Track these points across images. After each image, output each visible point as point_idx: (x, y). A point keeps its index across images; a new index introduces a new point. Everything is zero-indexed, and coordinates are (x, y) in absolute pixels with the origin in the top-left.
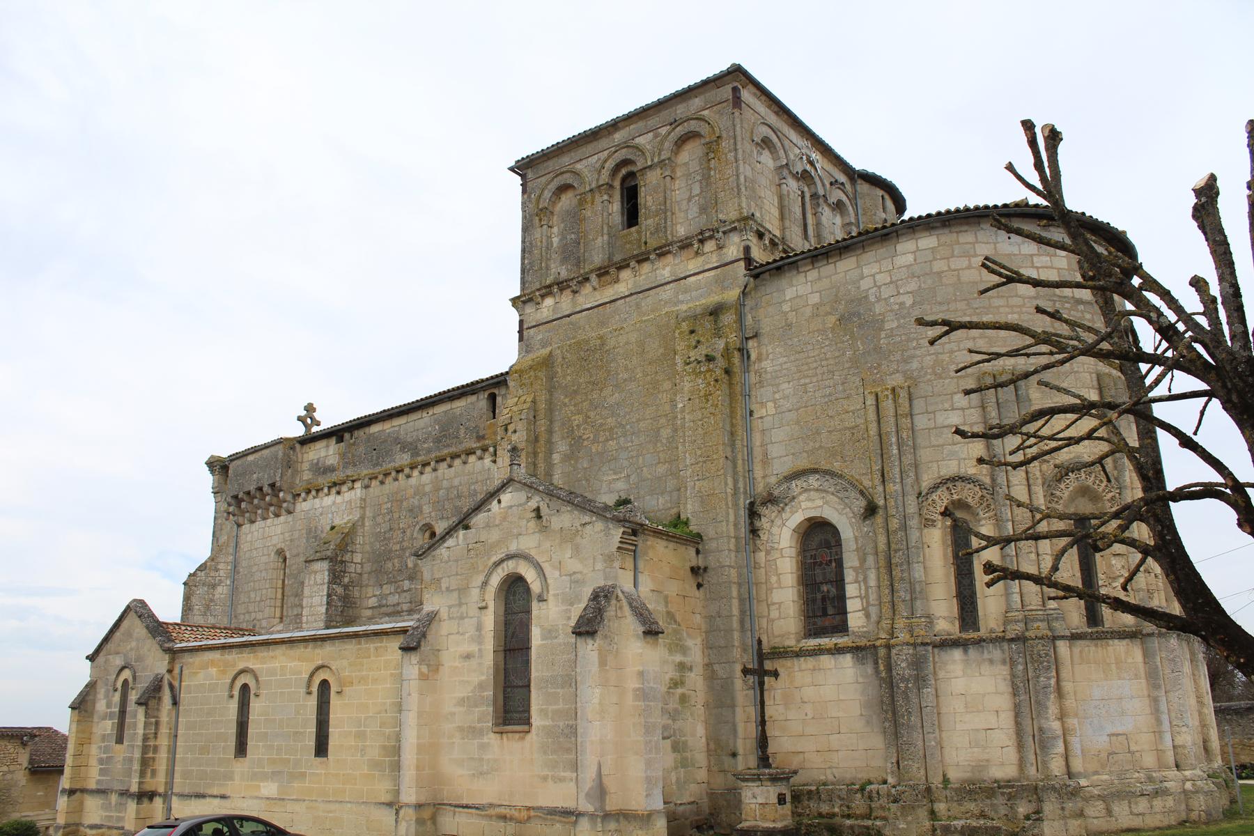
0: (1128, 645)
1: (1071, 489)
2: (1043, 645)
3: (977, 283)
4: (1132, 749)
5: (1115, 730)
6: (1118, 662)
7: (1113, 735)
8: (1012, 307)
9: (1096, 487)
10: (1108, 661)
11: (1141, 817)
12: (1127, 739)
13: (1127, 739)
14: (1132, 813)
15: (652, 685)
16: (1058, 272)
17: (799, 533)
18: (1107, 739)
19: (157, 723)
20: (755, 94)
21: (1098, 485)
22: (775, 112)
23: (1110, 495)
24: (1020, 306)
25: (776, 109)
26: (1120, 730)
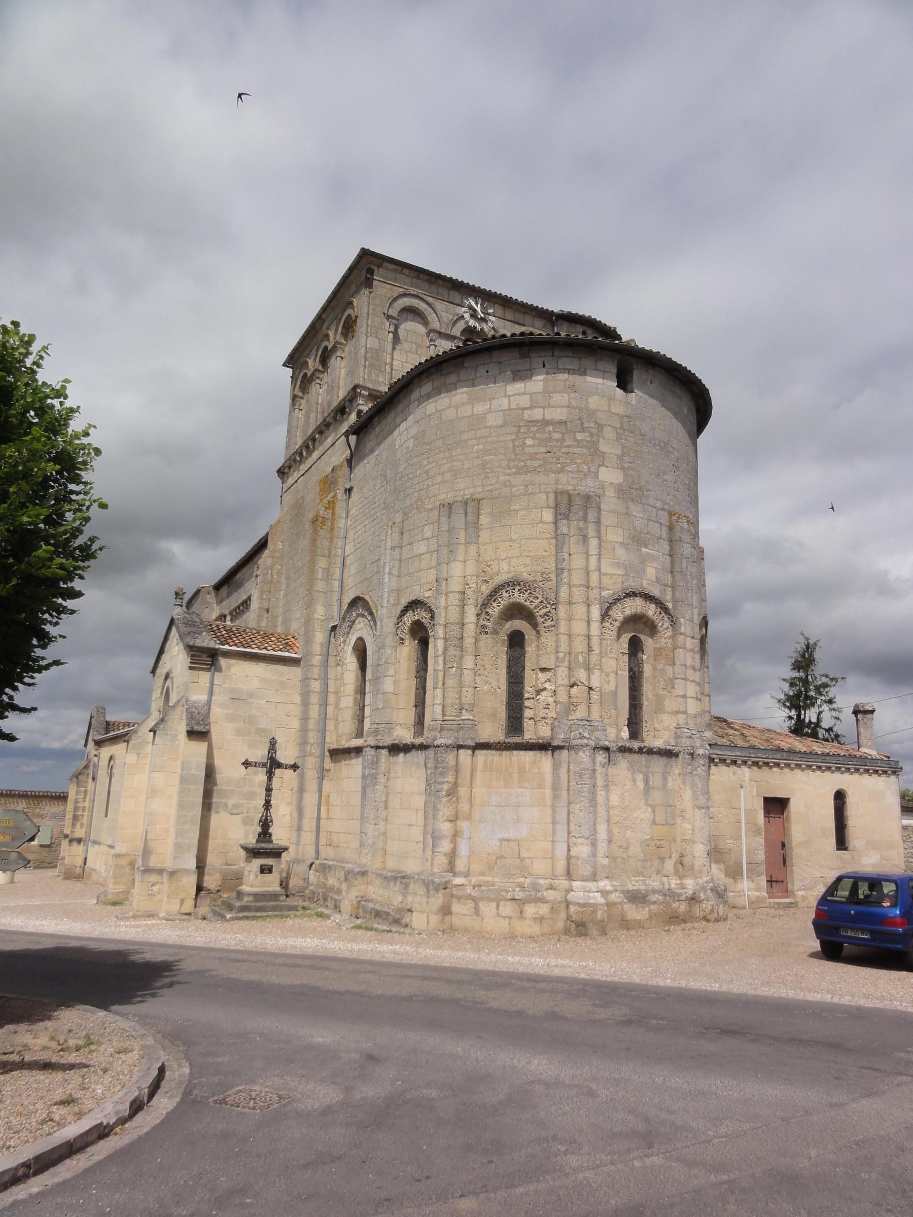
0: (535, 755)
1: (502, 607)
2: (441, 752)
3: (452, 421)
4: (521, 854)
5: (506, 836)
6: (521, 771)
7: (505, 840)
8: (480, 438)
9: (528, 603)
10: (511, 770)
11: (507, 920)
12: (519, 845)
13: (519, 845)
14: (498, 915)
15: (193, 772)
16: (531, 396)
17: (358, 650)
18: (498, 843)
19: (86, 792)
20: (395, 271)
21: (532, 602)
22: (427, 280)
23: (544, 611)
24: (486, 437)
25: (426, 277)
26: (512, 835)
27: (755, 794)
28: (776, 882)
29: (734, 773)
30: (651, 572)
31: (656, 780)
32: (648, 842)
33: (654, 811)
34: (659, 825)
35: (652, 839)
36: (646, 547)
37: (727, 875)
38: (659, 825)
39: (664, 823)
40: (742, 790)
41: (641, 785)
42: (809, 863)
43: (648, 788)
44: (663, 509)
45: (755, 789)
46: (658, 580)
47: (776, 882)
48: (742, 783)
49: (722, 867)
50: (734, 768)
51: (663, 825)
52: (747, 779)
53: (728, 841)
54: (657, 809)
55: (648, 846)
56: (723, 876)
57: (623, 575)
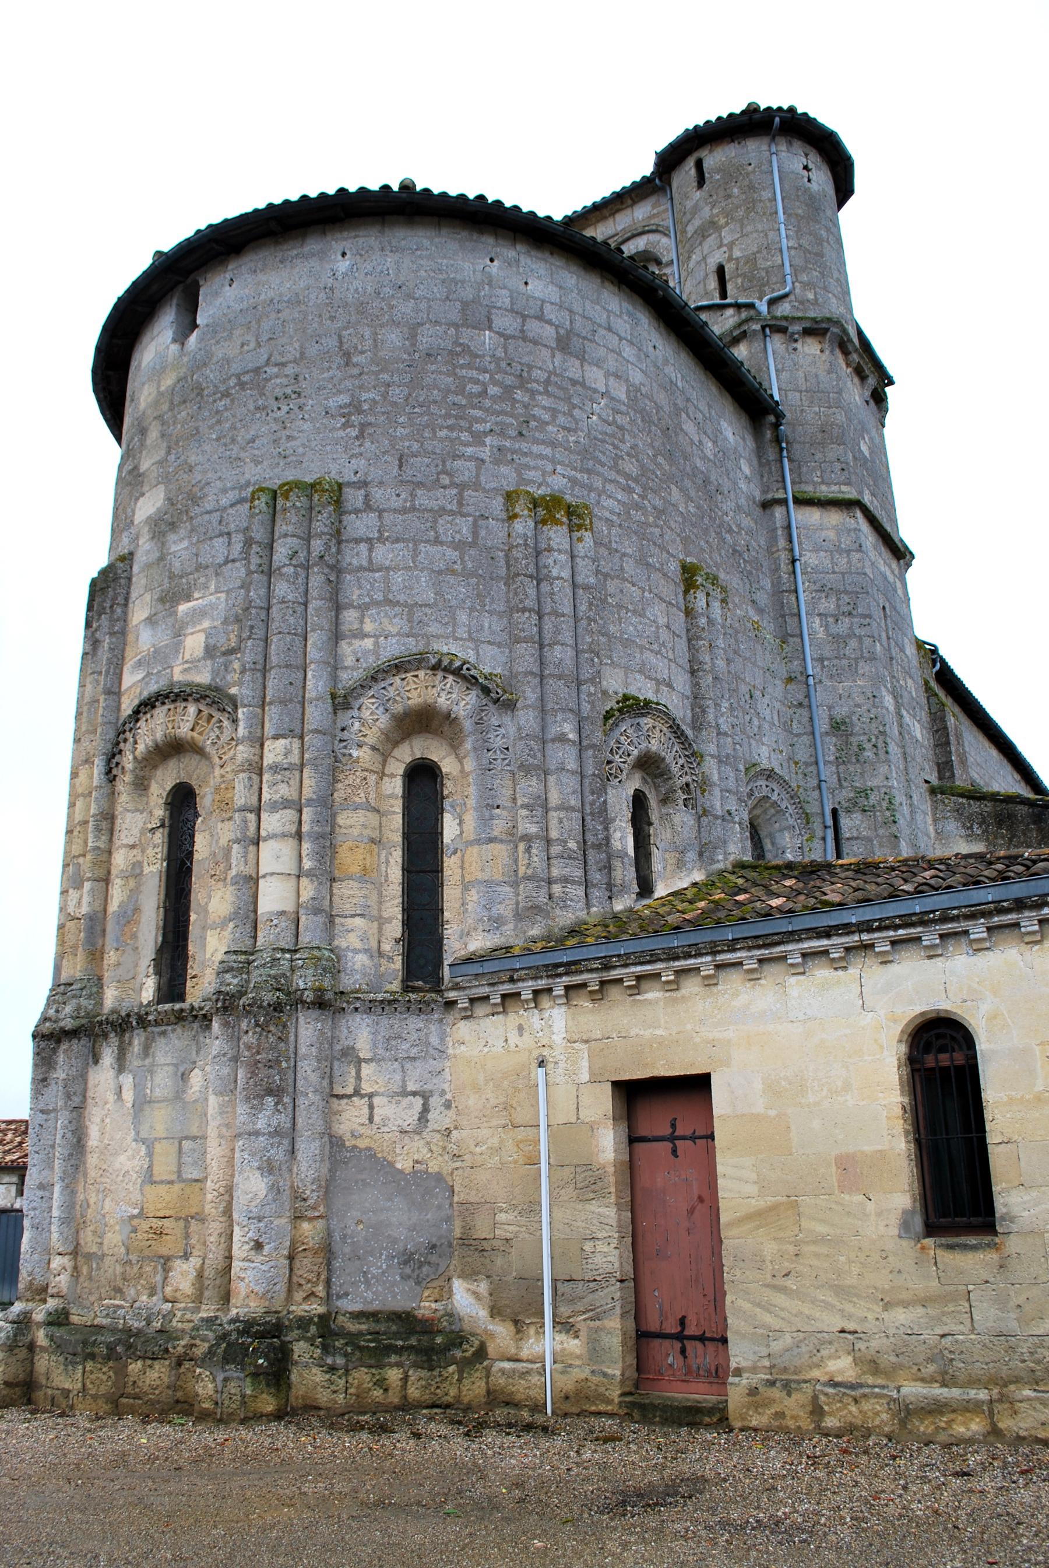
27: (585, 1077)
28: (702, 1339)
29: (520, 1028)
30: (194, 643)
31: (162, 1082)
32: (135, 1222)
33: (150, 1154)
34: (162, 1182)
35: (142, 1215)
36: (188, 598)
37: (495, 1312)
38: (162, 1182)
39: (174, 1177)
40: (541, 1071)
41: (128, 1096)
42: (790, 1283)
43: (141, 1104)
44: (241, 501)
45: (585, 1064)
46: (210, 651)
47: (702, 1339)
48: (546, 1052)
49: (483, 1287)
50: (515, 1017)
51: (171, 1182)
52: (558, 1038)
53: (502, 1217)
54: (158, 1148)
55: (135, 1231)
56: (483, 1313)
57: (143, 678)
